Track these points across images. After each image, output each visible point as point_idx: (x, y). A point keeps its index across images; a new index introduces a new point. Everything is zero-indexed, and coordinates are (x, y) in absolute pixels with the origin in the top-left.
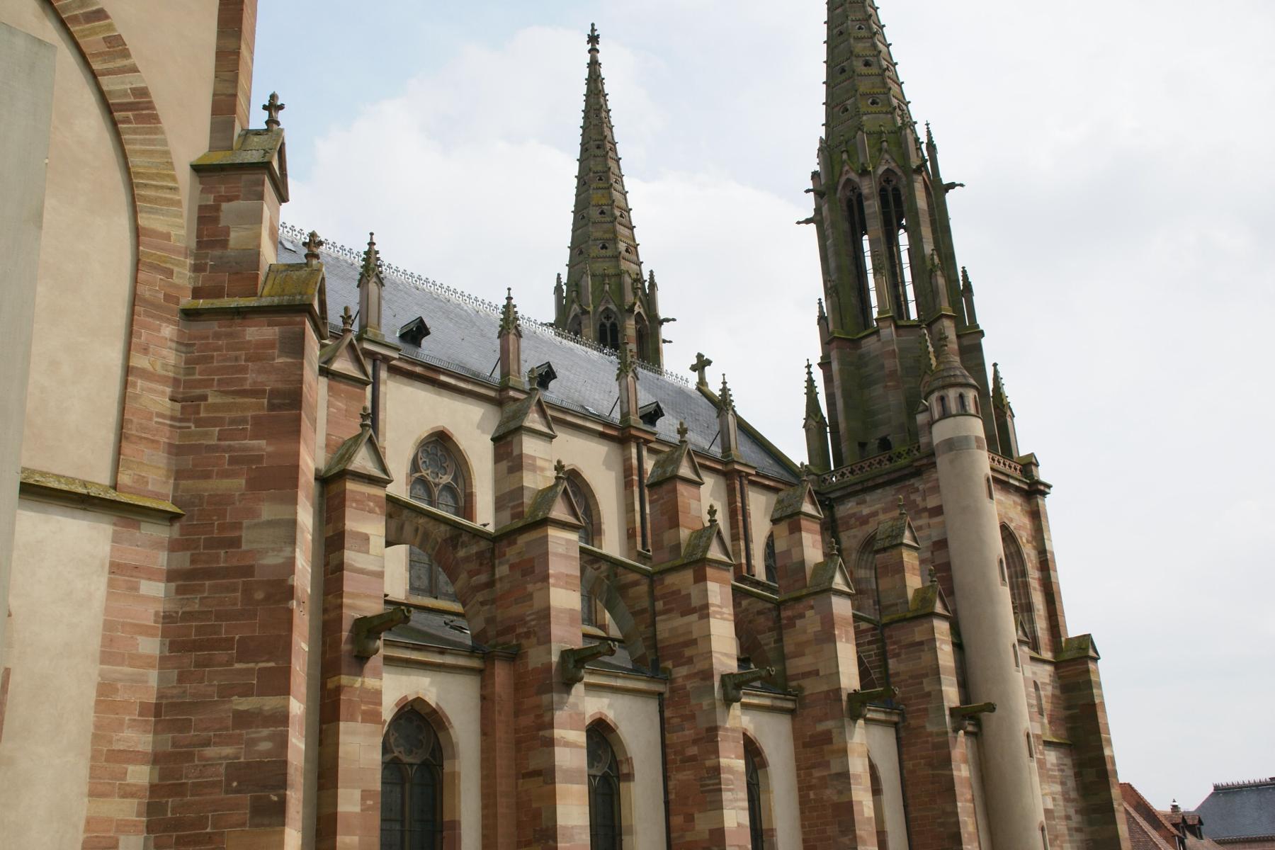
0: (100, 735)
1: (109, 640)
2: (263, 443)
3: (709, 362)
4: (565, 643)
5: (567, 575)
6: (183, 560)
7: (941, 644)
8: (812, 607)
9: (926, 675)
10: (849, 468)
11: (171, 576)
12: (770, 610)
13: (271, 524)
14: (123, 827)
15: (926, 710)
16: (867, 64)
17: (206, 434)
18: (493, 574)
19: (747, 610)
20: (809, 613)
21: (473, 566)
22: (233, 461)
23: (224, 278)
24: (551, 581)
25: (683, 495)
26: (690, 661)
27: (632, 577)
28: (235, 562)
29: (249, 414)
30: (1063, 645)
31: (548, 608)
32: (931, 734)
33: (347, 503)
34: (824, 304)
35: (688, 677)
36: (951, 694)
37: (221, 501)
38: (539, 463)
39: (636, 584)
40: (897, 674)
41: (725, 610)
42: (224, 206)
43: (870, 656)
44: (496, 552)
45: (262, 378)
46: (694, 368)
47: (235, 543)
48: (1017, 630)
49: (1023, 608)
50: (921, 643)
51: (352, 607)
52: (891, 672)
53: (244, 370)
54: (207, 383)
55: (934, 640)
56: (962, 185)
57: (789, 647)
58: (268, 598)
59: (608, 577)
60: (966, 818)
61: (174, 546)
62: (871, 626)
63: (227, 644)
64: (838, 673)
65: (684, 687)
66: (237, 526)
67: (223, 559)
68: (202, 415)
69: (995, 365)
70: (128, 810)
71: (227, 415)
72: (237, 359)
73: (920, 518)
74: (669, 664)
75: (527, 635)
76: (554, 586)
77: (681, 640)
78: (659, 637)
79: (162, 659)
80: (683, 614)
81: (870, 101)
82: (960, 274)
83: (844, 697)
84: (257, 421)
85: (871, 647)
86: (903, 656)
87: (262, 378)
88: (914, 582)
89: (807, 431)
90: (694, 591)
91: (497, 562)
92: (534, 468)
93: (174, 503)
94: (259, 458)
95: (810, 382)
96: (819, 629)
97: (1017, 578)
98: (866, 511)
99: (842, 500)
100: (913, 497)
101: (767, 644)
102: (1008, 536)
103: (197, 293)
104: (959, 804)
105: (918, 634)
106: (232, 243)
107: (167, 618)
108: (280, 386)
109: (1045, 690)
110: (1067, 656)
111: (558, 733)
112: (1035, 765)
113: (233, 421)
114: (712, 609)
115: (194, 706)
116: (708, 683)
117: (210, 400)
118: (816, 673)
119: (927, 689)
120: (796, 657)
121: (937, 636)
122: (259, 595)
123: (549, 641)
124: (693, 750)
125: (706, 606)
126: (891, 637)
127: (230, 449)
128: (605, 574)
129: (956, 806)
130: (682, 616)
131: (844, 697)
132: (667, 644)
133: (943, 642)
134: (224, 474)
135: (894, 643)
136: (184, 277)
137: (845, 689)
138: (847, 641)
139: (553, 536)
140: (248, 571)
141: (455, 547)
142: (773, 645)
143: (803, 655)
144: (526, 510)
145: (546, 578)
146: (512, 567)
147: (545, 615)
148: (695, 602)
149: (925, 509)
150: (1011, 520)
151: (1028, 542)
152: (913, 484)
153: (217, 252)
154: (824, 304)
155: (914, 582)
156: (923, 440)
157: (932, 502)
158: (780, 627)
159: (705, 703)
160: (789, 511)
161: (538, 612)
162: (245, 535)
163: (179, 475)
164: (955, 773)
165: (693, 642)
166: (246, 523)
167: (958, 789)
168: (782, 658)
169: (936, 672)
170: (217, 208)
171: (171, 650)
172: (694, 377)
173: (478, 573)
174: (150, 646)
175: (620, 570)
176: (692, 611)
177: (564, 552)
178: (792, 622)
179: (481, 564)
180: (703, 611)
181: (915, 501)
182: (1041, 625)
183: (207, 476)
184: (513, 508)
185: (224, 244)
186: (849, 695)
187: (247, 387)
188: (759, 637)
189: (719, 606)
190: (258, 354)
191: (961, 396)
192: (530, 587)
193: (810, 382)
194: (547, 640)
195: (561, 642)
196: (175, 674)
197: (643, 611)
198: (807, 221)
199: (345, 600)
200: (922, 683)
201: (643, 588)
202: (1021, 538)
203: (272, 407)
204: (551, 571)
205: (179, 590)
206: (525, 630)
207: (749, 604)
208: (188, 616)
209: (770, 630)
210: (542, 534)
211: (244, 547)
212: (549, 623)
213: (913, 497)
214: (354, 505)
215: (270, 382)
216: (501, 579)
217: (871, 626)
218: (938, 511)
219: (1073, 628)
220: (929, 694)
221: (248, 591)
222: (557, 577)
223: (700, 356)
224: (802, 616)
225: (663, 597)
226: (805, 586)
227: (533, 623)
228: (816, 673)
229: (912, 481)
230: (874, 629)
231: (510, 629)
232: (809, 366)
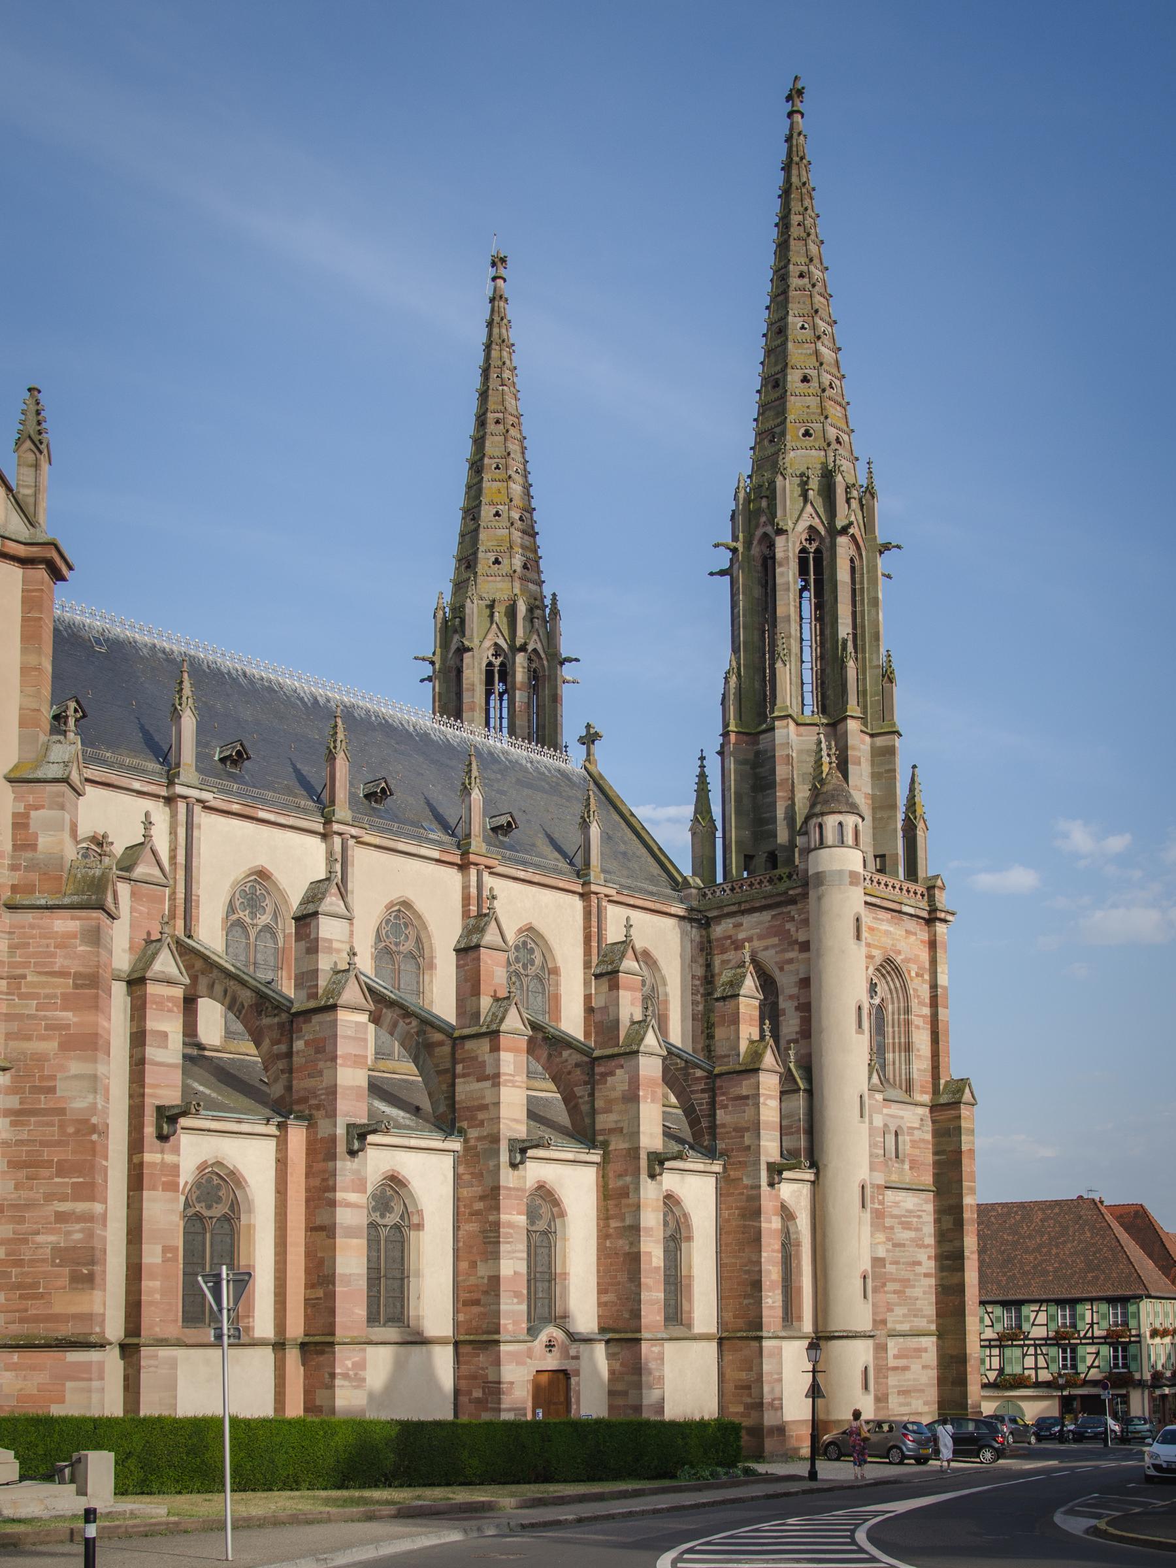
2: (69, 1014)
4: (351, 1116)
5: (355, 1055)
7: (766, 1099)
8: (622, 1067)
9: (747, 1129)
10: (730, 885)
12: (587, 1063)
13: (76, 1077)
15: (745, 1162)
18: (292, 1047)
19: (567, 1061)
20: (618, 1072)
21: (275, 1034)
24: (339, 1061)
25: (486, 963)
26: (481, 1124)
27: (438, 1037)
28: (51, 1105)
29: (59, 991)
30: (941, 1087)
31: (336, 1085)
32: (746, 1187)
33: (148, 1006)
35: (479, 1139)
37: (40, 1059)
38: (336, 945)
39: (441, 1044)
40: (723, 1126)
41: (517, 1078)
43: (702, 1104)
44: (295, 1026)
45: (67, 962)
47: (52, 1090)
48: (870, 1078)
50: (747, 1097)
51: (152, 1096)
52: (718, 1122)
53: (53, 955)
57: (599, 1104)
59: (418, 1034)
60: (771, 1268)
62: (706, 1074)
64: (638, 1132)
67: (43, 1102)
68: (23, 990)
71: (42, 991)
72: (48, 946)
73: (793, 950)
74: (465, 1124)
75: (318, 1107)
76: (342, 1065)
78: (457, 1098)
84: (65, 997)
85: (703, 1095)
86: (730, 1108)
88: (749, 1031)
89: (693, 834)
90: (488, 1058)
91: (294, 1036)
92: (330, 950)
95: (702, 777)
96: (627, 1088)
97: (899, 1014)
98: (741, 936)
99: (718, 919)
100: (788, 926)
101: (581, 1097)
104: (764, 1254)
105: (745, 1088)
108: (81, 969)
110: (944, 1099)
111: (339, 1195)
112: (867, 1216)
113: (47, 996)
114: (502, 1079)
116: (495, 1146)
117: (29, 978)
120: (605, 1113)
121: (761, 1091)
123: (335, 1116)
125: (497, 1075)
126: (721, 1087)
127: (45, 1018)
128: (415, 1030)
129: (760, 1257)
130: (478, 1081)
131: (643, 1156)
132: (464, 1105)
133: (770, 1097)
134: (42, 1038)
137: (646, 1148)
138: (653, 1101)
139: (342, 1020)
141: (260, 1013)
142: (586, 1098)
143: (611, 1112)
144: (320, 991)
145: (334, 1059)
146: (307, 1044)
147: (332, 1091)
148: (489, 1070)
149: (796, 942)
150: (899, 953)
152: (790, 912)
158: (592, 1082)
160: (610, 968)
161: (327, 1088)
162: (59, 1085)
164: (764, 1225)
165: (484, 1107)
166: (59, 1075)
167: (765, 1240)
168: (593, 1112)
169: (755, 1127)
171: (9, 1167)
173: (278, 1042)
175: (429, 1029)
176: (487, 1078)
177: (353, 1035)
178: (604, 1075)
179: (282, 1035)
180: (495, 1079)
183: (29, 1038)
184: (310, 987)
186: (649, 1154)
187: (57, 969)
188: (575, 1089)
189: (511, 1075)
190: (64, 943)
192: (321, 1065)
193: (702, 777)
194: (332, 1115)
195: (346, 1116)
197: (446, 1071)
199: (146, 1090)
200: (743, 1137)
201: (447, 1049)
202: (909, 972)
203: (76, 986)
204: (339, 1053)
205: (13, 1124)
206: (316, 1102)
207: (570, 1055)
209: (586, 1083)
210: (332, 1018)
211: (59, 1094)
212: (336, 1099)
213: (788, 926)
214: (154, 1007)
215: (75, 967)
216: (298, 1052)
217: (706, 1074)
218: (805, 947)
219: (954, 1069)
222: (344, 1057)
224: (612, 1074)
226: (618, 1045)
227: (323, 1097)
229: (789, 908)
230: (707, 1078)
231: (304, 1100)
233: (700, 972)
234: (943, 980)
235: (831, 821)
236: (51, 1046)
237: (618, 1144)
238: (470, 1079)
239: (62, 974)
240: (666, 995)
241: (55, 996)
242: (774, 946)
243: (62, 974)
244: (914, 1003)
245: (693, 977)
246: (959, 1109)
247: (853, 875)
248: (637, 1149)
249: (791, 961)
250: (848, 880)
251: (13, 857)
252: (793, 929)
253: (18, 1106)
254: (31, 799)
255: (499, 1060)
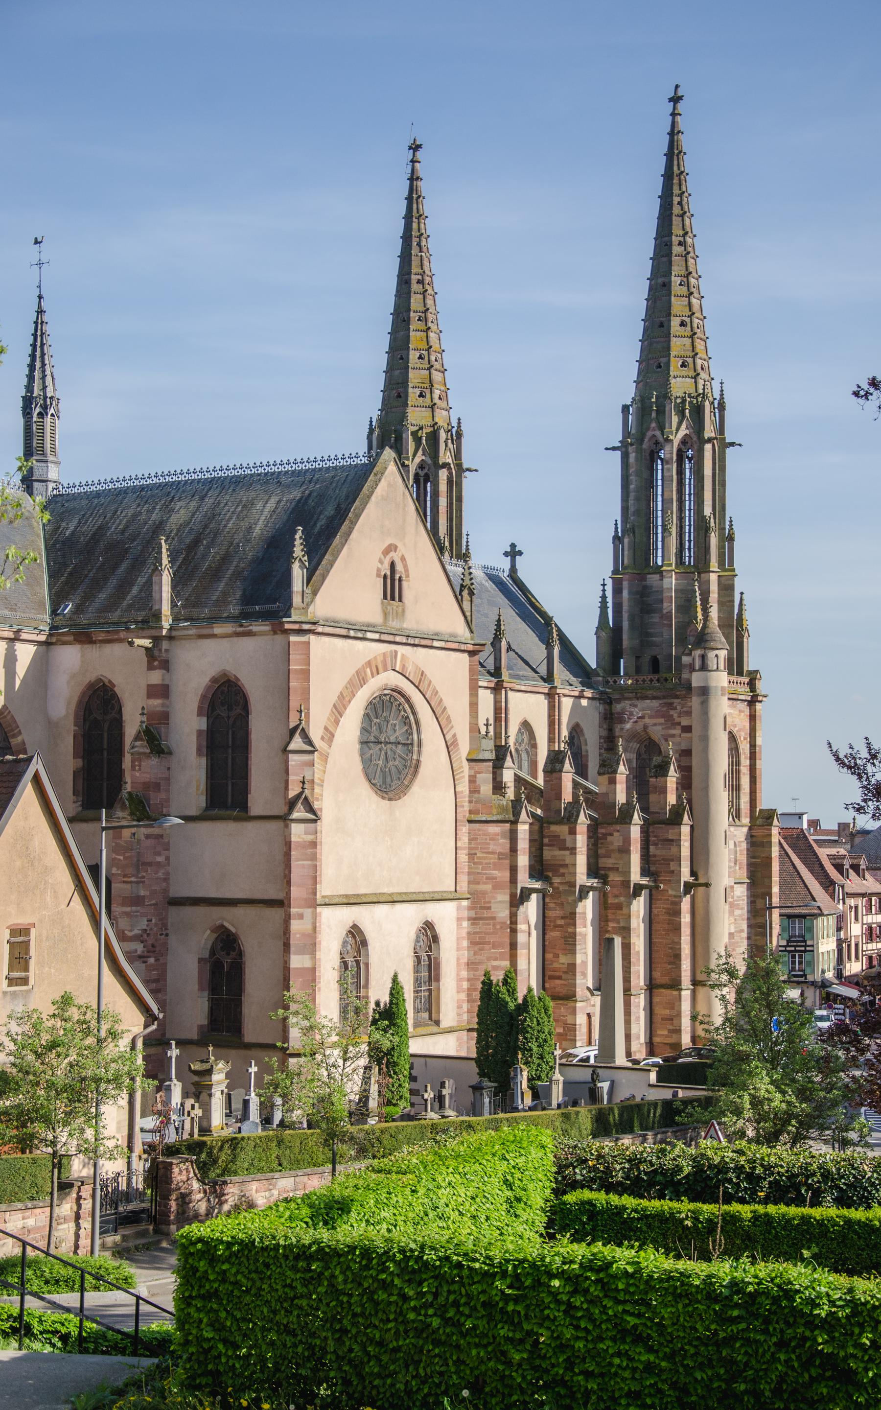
0: (458, 975)
1: (458, 944)
3: (520, 553)
6: (473, 914)
8: (618, 831)
9: (672, 860)
11: (469, 919)
13: (500, 902)
14: (463, 1001)
16: (683, 324)
17: (477, 868)
20: (616, 834)
22: (487, 878)
23: (479, 806)
28: (489, 915)
32: (671, 896)
34: (619, 526)
36: (685, 875)
37: (484, 893)
40: (655, 856)
42: (478, 775)
45: (495, 847)
46: (506, 554)
47: (489, 908)
49: (735, 788)
50: (672, 840)
53: (488, 844)
54: (476, 848)
55: (680, 840)
56: (740, 445)
58: (501, 928)
61: (470, 908)
63: (489, 943)
64: (630, 872)
65: (558, 888)
66: (490, 902)
67: (486, 914)
69: (742, 593)
70: (463, 996)
73: (675, 729)
74: (550, 874)
77: (558, 863)
79: (468, 947)
80: (560, 849)
81: (680, 363)
82: (727, 523)
83: (632, 886)
84: (494, 864)
87: (495, 847)
88: (672, 799)
90: (569, 838)
93: (469, 893)
94: (496, 878)
95: (604, 597)
99: (618, 701)
102: (732, 738)
103: (470, 812)
104: (682, 938)
106: (482, 792)
107: (469, 933)
109: (740, 846)
112: (727, 907)
114: (578, 850)
115: (479, 963)
118: (617, 869)
119: (672, 869)
122: (498, 927)
124: (560, 922)
125: (575, 848)
127: (486, 874)
131: (632, 886)
134: (485, 883)
135: (655, 836)
136: (466, 807)
140: (494, 918)
148: (569, 844)
150: (735, 726)
151: (745, 739)
153: (476, 795)
154: (619, 526)
155: (672, 799)
156: (685, 676)
157: (685, 722)
159: (570, 899)
162: (493, 906)
163: (469, 883)
165: (566, 866)
169: (679, 859)
170: (475, 777)
172: (506, 564)
174: (465, 943)
176: (567, 849)
178: (605, 836)
180: (573, 850)
181: (672, 716)
182: (745, 799)
183: (478, 883)
185: (478, 792)
186: (635, 884)
187: (490, 850)
191: (717, 656)
193: (604, 597)
196: (472, 952)
198: (614, 449)
203: (499, 859)
205: (473, 924)
208: (475, 933)
213: (672, 712)
215: (499, 849)
218: (688, 729)
220: (673, 872)
221: (494, 925)
223: (513, 546)
224: (611, 835)
225: (548, 837)
228: (617, 869)
232: (604, 585)
233: (604, 733)
234: (759, 741)
235: (711, 654)
236: (488, 887)
237: (613, 877)
238: (555, 848)
239: (493, 853)
240: (587, 751)
241: (490, 863)
242: (661, 724)
243: (493, 853)
244: (742, 757)
245: (600, 737)
246: (771, 830)
247: (723, 688)
248: (630, 881)
249: (673, 736)
250: (720, 693)
251: (469, 797)
252: (675, 715)
253: (474, 916)
254: (477, 768)
255: (576, 840)
